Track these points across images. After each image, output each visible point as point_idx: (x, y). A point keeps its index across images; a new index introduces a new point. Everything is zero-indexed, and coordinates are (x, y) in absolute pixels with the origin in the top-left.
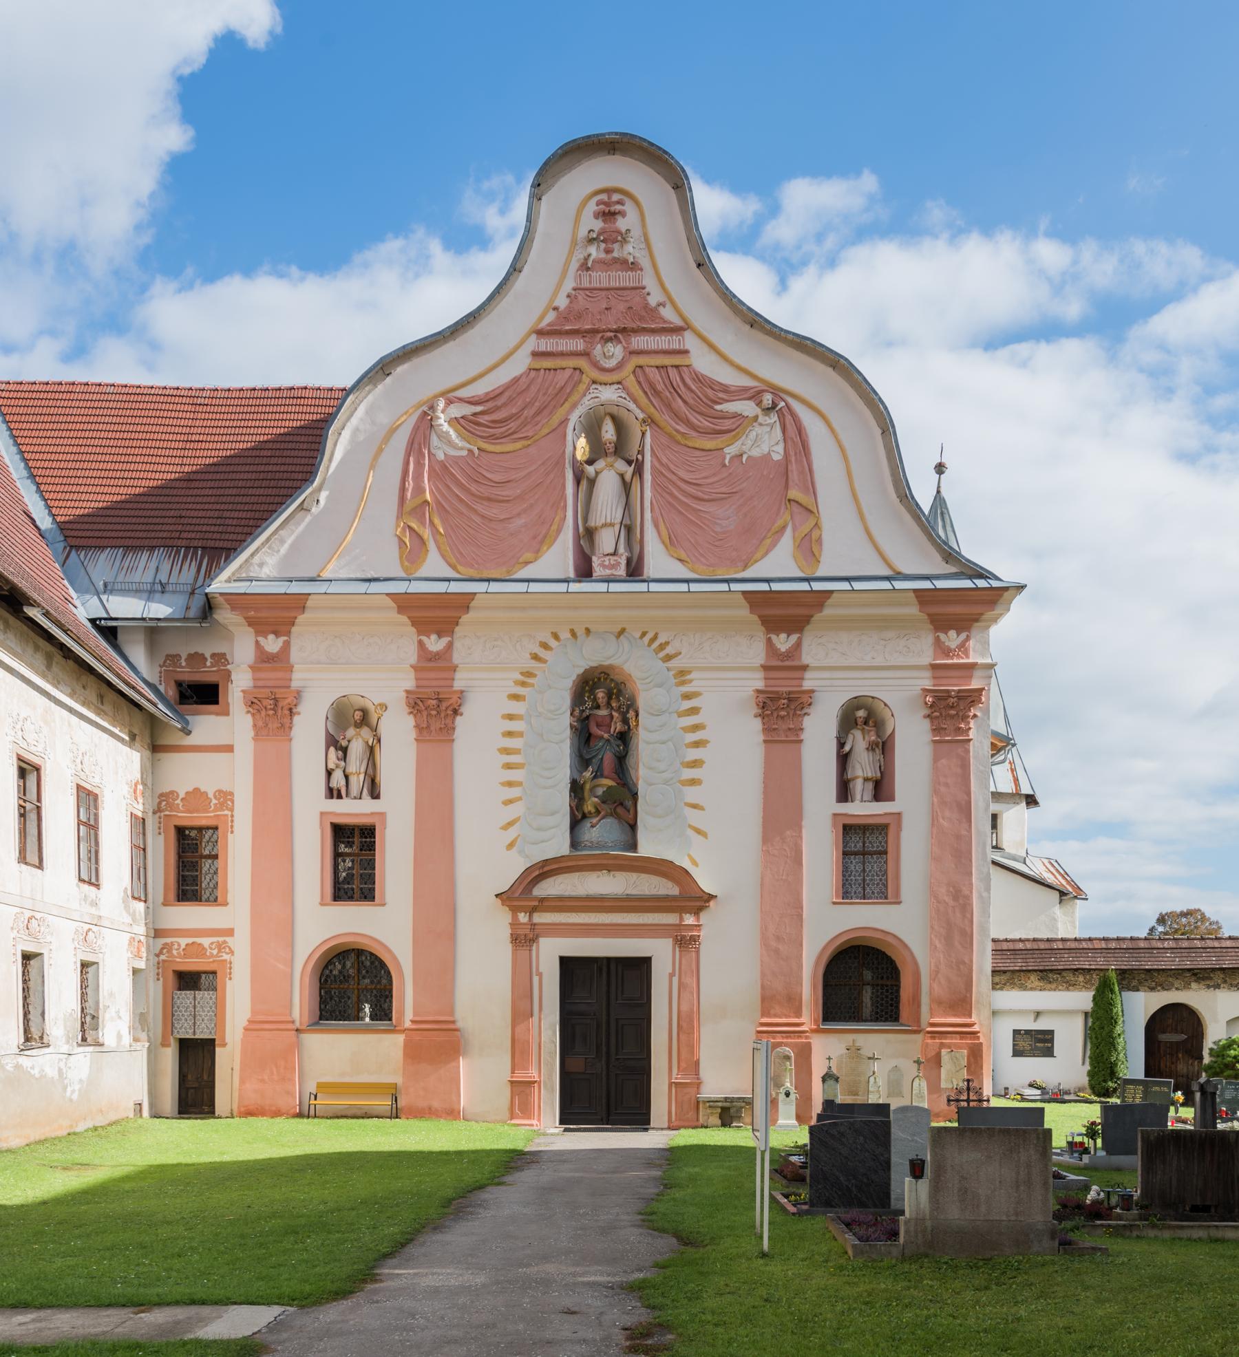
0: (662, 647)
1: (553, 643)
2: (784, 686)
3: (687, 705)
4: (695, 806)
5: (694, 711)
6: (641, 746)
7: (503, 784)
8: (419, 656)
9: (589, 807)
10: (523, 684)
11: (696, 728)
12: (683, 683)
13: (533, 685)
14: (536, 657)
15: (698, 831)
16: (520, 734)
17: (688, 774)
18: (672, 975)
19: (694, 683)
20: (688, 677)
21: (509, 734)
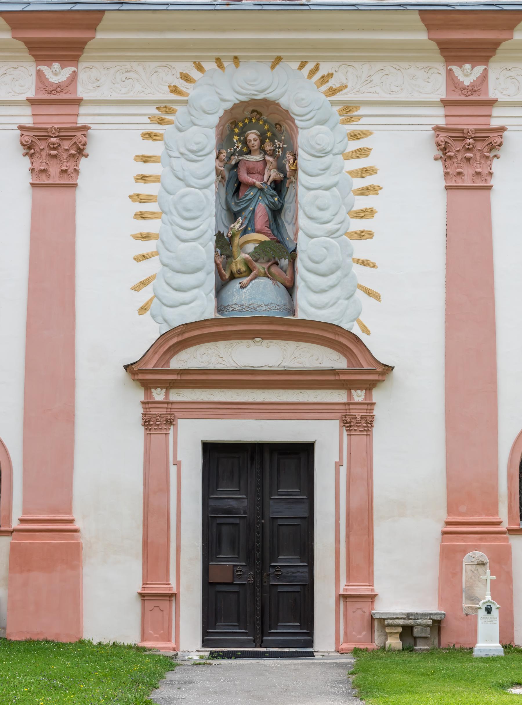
0: (324, 79)
1: (195, 74)
2: (468, 122)
3: (354, 145)
4: (364, 263)
5: (363, 153)
6: (301, 190)
7: (135, 237)
8: (38, 89)
9: (238, 265)
10: (161, 121)
11: (365, 172)
12: (349, 121)
13: (171, 123)
14: (175, 90)
15: (369, 293)
16: (156, 179)
17: (357, 225)
18: (338, 465)
19: (363, 121)
20: (356, 113)
21: (144, 178)
